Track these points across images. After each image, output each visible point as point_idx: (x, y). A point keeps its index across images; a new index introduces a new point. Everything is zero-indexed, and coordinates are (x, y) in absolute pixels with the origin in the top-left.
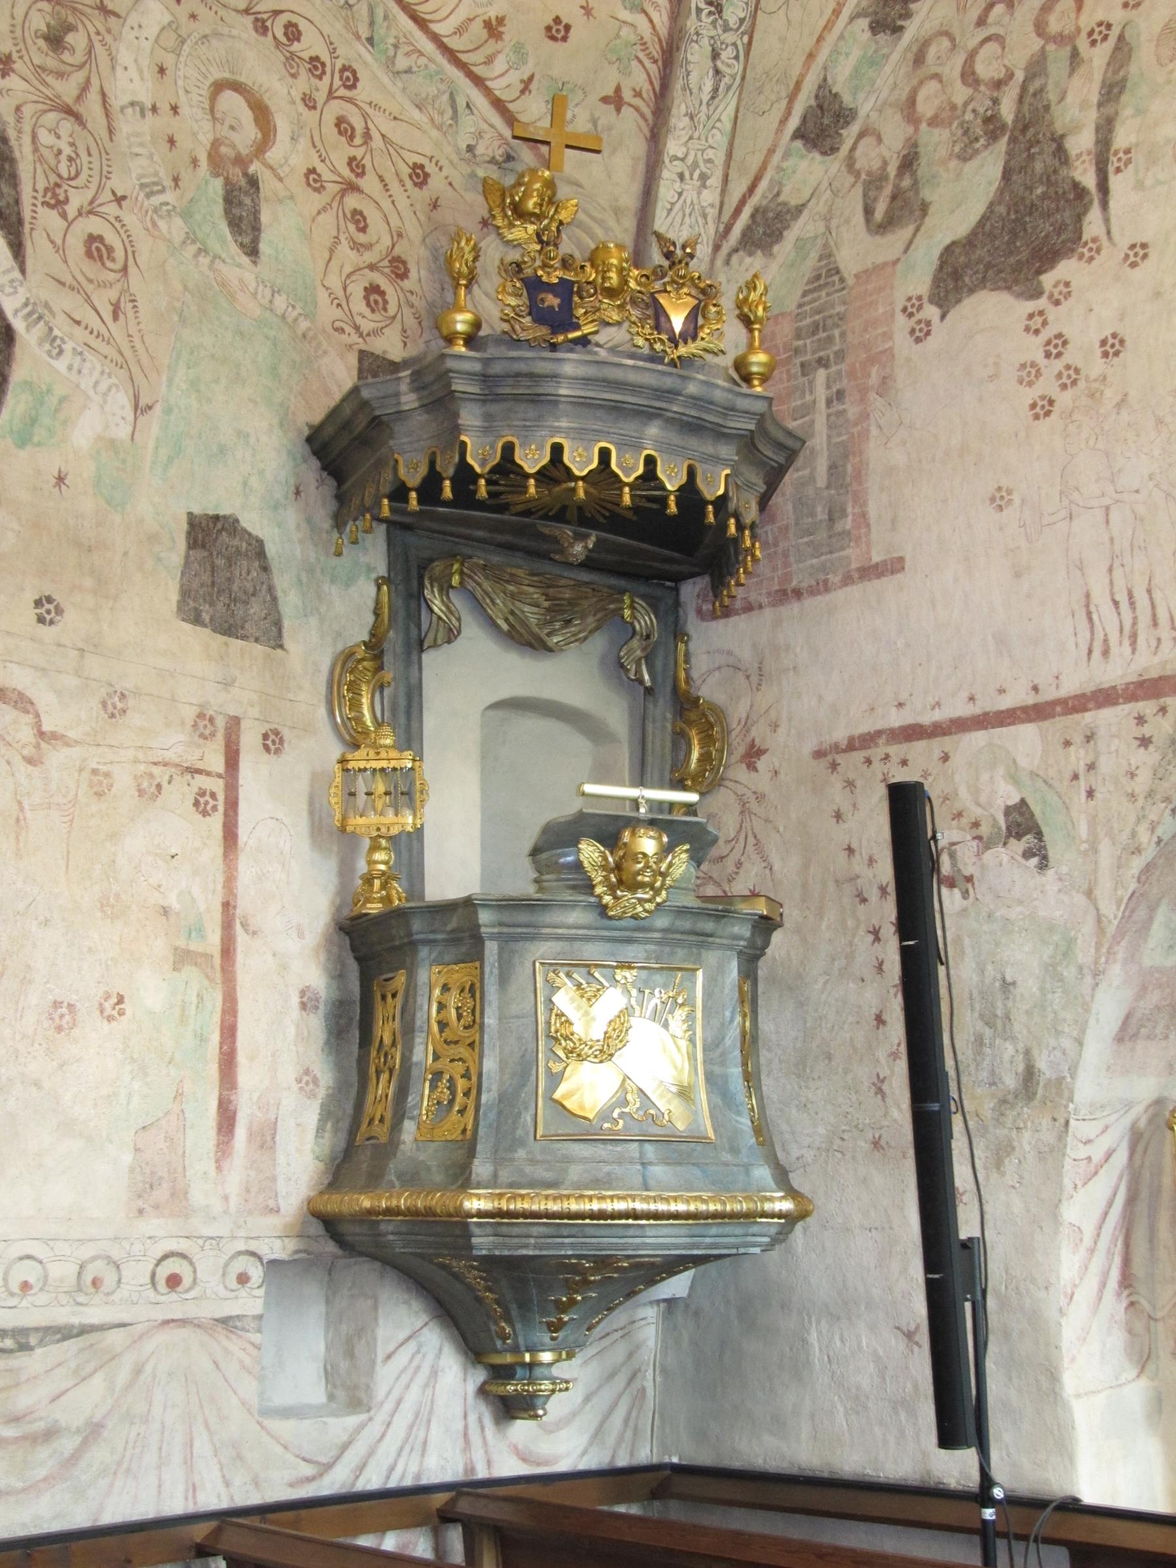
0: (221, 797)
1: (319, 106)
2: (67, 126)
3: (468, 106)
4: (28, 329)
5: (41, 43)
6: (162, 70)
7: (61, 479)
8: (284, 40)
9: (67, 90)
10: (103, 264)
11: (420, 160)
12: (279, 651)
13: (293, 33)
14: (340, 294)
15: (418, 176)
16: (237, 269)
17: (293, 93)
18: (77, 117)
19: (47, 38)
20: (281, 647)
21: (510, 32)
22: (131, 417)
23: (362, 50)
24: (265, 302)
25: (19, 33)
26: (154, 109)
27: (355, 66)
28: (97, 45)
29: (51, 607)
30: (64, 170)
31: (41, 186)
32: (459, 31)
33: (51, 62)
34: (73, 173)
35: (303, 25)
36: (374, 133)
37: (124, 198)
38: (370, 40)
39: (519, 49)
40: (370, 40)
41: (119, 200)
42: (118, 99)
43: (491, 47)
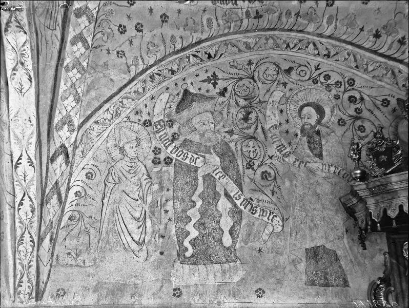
2: (251, 143)
3: (400, 72)
4: (245, 208)
5: (242, 121)
7: (260, 250)
8: (325, 81)
9: (251, 131)
10: (267, 179)
11: (384, 97)
12: (347, 288)
13: (327, 77)
15: (385, 103)
16: (315, 164)
17: (330, 97)
18: (255, 138)
19: (243, 119)
20: (348, 286)
22: (281, 223)
23: (355, 71)
24: (327, 171)
25: (235, 122)
27: (353, 77)
28: (259, 114)
29: (261, 292)
30: (252, 156)
31: (245, 164)
32: (389, 48)
34: (255, 155)
35: (330, 73)
36: (365, 97)
37: (273, 156)
40: (357, 67)
41: (271, 158)
42: (267, 127)
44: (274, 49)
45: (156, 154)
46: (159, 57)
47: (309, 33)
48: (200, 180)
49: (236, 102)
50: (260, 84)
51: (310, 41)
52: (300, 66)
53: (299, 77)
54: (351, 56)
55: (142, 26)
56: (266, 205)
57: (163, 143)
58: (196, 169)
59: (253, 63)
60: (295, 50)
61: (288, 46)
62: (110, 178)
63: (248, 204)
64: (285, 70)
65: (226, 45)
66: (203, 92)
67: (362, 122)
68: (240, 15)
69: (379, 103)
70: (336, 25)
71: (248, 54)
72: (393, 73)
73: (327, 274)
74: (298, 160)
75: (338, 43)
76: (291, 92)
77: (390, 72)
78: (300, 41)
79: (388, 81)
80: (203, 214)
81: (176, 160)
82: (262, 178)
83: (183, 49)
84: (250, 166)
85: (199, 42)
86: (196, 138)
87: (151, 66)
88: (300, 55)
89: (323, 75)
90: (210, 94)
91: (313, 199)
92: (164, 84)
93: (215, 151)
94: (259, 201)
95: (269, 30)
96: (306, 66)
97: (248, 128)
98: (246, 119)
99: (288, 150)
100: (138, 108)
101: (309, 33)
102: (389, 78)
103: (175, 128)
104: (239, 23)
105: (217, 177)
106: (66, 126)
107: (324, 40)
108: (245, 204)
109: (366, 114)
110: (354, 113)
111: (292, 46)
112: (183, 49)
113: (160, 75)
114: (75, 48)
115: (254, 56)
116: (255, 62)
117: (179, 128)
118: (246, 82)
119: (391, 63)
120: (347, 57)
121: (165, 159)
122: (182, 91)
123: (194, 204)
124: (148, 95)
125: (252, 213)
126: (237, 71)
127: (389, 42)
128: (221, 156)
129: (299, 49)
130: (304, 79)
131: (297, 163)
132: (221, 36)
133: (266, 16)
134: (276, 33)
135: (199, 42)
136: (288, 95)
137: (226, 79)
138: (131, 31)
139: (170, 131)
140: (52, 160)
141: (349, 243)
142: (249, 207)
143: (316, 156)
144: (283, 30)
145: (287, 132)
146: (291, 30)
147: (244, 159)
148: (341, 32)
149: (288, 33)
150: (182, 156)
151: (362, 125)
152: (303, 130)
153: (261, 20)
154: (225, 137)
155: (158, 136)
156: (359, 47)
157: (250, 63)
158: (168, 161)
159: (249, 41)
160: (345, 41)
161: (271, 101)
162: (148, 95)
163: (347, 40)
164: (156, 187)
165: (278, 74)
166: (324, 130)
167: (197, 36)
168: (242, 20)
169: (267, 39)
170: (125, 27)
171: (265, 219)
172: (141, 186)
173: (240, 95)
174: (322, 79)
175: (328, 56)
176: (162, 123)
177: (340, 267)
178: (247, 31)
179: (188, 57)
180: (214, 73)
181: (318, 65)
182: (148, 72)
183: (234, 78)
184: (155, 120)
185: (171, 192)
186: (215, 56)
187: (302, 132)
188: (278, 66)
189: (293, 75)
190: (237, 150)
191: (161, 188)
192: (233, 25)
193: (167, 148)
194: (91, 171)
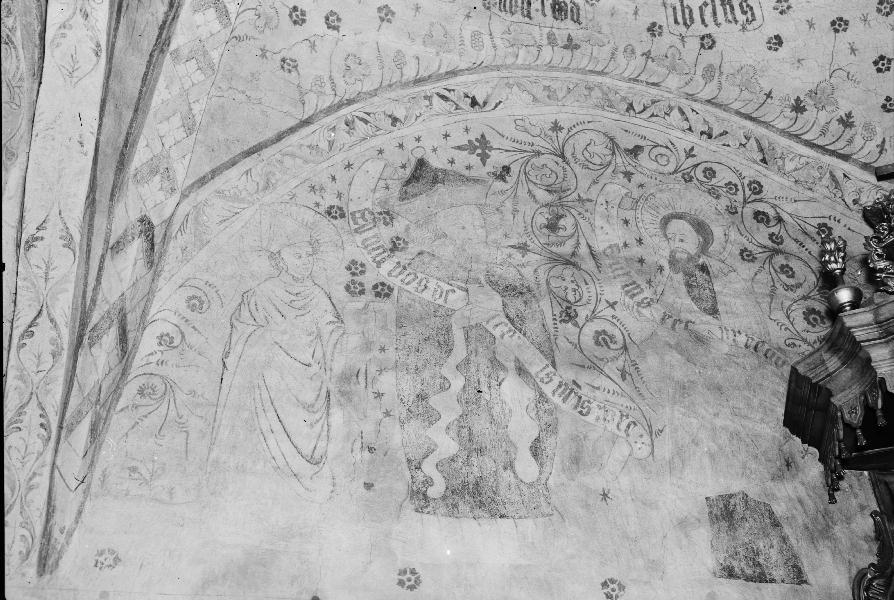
1: (739, 210)
2: (568, 272)
3: (845, 176)
4: (564, 401)
5: (545, 231)
6: (626, 222)
8: (705, 180)
9: (566, 249)
10: (609, 348)
12: (804, 585)
13: (710, 173)
14: (786, 322)
15: (824, 232)
17: (719, 207)
18: (574, 265)
19: (547, 227)
20: (805, 582)
21: (858, 119)
24: (730, 341)
25: (530, 229)
26: (626, 245)
28: (581, 221)
29: (615, 586)
30: (571, 298)
31: (557, 312)
32: (823, 133)
33: (553, 238)
35: (716, 167)
36: (785, 217)
37: (615, 303)
38: (764, 161)
39: (868, 127)
40: (764, 161)
41: (612, 305)
43: (849, 133)
44: (604, 109)
45: (354, 274)
49: (529, 191)
50: (578, 169)
51: (673, 104)
53: (654, 166)
54: (752, 141)
55: (339, 19)
57: (369, 253)
59: (561, 129)
61: (631, 107)
62: (245, 314)
63: (570, 394)
64: (627, 150)
66: (459, 167)
67: (786, 259)
68: (538, 38)
69: (812, 230)
71: (554, 109)
72: (833, 177)
74: (670, 317)
76: (641, 191)
77: (828, 175)
78: (653, 102)
81: (400, 289)
82: (597, 343)
83: (418, 81)
85: (453, 73)
88: (651, 125)
90: (473, 173)
96: (667, 147)
97: (562, 244)
98: (552, 226)
100: (316, 181)
103: (399, 227)
104: (534, 50)
105: (497, 333)
106: (158, 178)
107: (697, 106)
108: (563, 393)
109: (789, 245)
111: (638, 108)
112: (418, 81)
113: (366, 122)
114: (199, 18)
116: (565, 125)
117: (407, 229)
119: (828, 159)
120: (744, 141)
121: (375, 287)
122: (413, 162)
123: (444, 386)
124: (339, 158)
125: (581, 412)
129: (652, 115)
133: (586, 48)
135: (453, 73)
136: (636, 193)
137: (507, 151)
138: (315, 24)
139: (386, 233)
140: (117, 248)
142: (573, 400)
145: (641, 261)
146: (635, 80)
147: (555, 303)
148: (730, 94)
149: (631, 85)
150: (415, 284)
151: (787, 266)
152: (673, 261)
153: (577, 53)
154: (510, 256)
156: (767, 125)
157: (556, 127)
161: (601, 200)
162: (339, 158)
163: (743, 111)
165: (614, 153)
166: (714, 266)
167: (451, 60)
168: (540, 47)
170: (303, 13)
171: (612, 427)
172: (319, 336)
173: (538, 182)
174: (700, 176)
180: (483, 136)
181: (692, 149)
182: (344, 111)
184: (353, 208)
186: (485, 103)
189: (643, 157)
193: (379, 264)
194: (199, 294)
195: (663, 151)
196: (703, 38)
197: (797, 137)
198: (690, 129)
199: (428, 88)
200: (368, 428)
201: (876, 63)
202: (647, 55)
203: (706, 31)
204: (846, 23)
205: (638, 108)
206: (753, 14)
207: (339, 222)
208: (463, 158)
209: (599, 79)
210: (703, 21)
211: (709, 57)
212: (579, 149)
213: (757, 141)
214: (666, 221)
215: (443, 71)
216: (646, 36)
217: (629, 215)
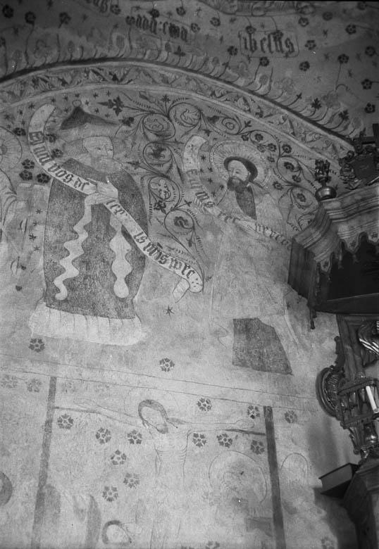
0: (265, 444)
1: (276, 160)
2: (162, 182)
3: (341, 148)
4: (150, 254)
7: (169, 310)
9: (163, 169)
10: (183, 226)
13: (259, 137)
14: (297, 225)
16: (247, 223)
17: (263, 157)
18: (168, 178)
19: (152, 154)
20: (290, 373)
22: (201, 282)
25: (141, 154)
26: (201, 170)
27: (289, 144)
29: (169, 363)
30: (163, 195)
31: (153, 202)
32: (330, 122)
33: (156, 161)
34: (167, 196)
35: (263, 134)
37: (191, 203)
38: (293, 133)
40: (293, 133)
41: (189, 204)
42: (184, 169)
43: (345, 123)
44: (196, 93)
45: (26, 167)
46: (49, 60)
47: (238, 87)
48: (88, 209)
49: (144, 133)
50: (176, 125)
52: (227, 117)
54: (287, 122)
56: (180, 255)
57: (38, 156)
58: (82, 196)
59: (168, 100)
60: (222, 99)
61: (213, 94)
63: (155, 250)
65: (138, 70)
67: (301, 191)
68: (159, 46)
70: (270, 86)
72: (334, 148)
73: (262, 354)
74: (225, 214)
75: (272, 105)
76: (215, 142)
77: (331, 147)
78: (228, 92)
79: (329, 155)
80: (88, 248)
81: (55, 180)
82: (176, 224)
84: (160, 206)
86: (86, 160)
87: (37, 69)
89: (254, 133)
90: (109, 119)
91: (244, 261)
92: (50, 94)
93: (111, 179)
94: (170, 249)
95: (191, 71)
96: (234, 119)
98: (157, 154)
99: (211, 200)
100: (10, 113)
101: (238, 87)
102: (329, 153)
103: (58, 145)
104: (156, 53)
105: (112, 211)
108: (150, 249)
109: (304, 183)
110: (292, 181)
111: (218, 95)
113: (46, 82)
115: (171, 93)
117: (64, 146)
118: (160, 118)
119: (332, 137)
120: (282, 121)
121: (39, 176)
122: (73, 108)
123: (75, 235)
125: (160, 262)
126: (148, 103)
127: (330, 114)
128: (121, 188)
130: (231, 132)
131: (223, 217)
132: (132, 60)
134: (200, 76)
136: (212, 143)
137: (133, 109)
139: (50, 146)
141: (291, 320)
143: (248, 214)
144: (209, 76)
145: (210, 181)
146: (218, 79)
147: (152, 198)
148: (276, 93)
149: (215, 81)
150: (64, 177)
151: (302, 194)
152: (230, 183)
153: (183, 58)
154: (127, 168)
155: (32, 148)
158: (43, 178)
159: (168, 75)
160: (279, 105)
162: (27, 101)
164: (22, 204)
165: (200, 119)
166: (256, 189)
168: (160, 52)
169: (189, 79)
171: (179, 272)
173: (150, 129)
174: (254, 139)
175: (260, 115)
176: (40, 135)
177: (281, 348)
178: (164, 64)
179: (88, 73)
180: (118, 98)
181: (249, 122)
182: (32, 74)
183: (144, 111)
184: (31, 130)
185: (44, 214)
187: (228, 184)
188: (200, 111)
189: (218, 124)
190: (142, 185)
191: (29, 206)
192: (148, 52)
195: (231, 121)
196: (261, 59)
197: (314, 123)
198: (249, 110)
199: (90, 66)
200: (23, 255)
201: (363, 83)
202: (226, 65)
203: (262, 55)
204: (348, 58)
205: (218, 95)
206: (293, 48)
207: (21, 138)
208: (104, 110)
209: (195, 75)
210: (262, 49)
211: (265, 71)
212: (179, 114)
213: (291, 122)
214: (228, 161)
215: (97, 57)
216: (227, 54)
217: (206, 154)
